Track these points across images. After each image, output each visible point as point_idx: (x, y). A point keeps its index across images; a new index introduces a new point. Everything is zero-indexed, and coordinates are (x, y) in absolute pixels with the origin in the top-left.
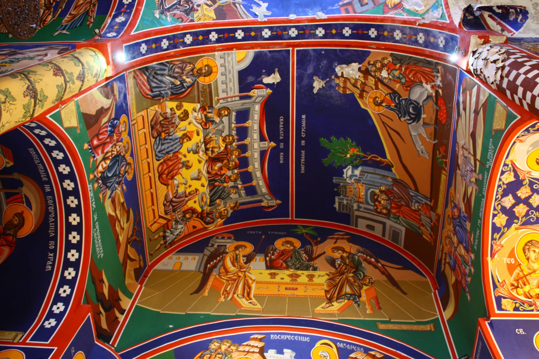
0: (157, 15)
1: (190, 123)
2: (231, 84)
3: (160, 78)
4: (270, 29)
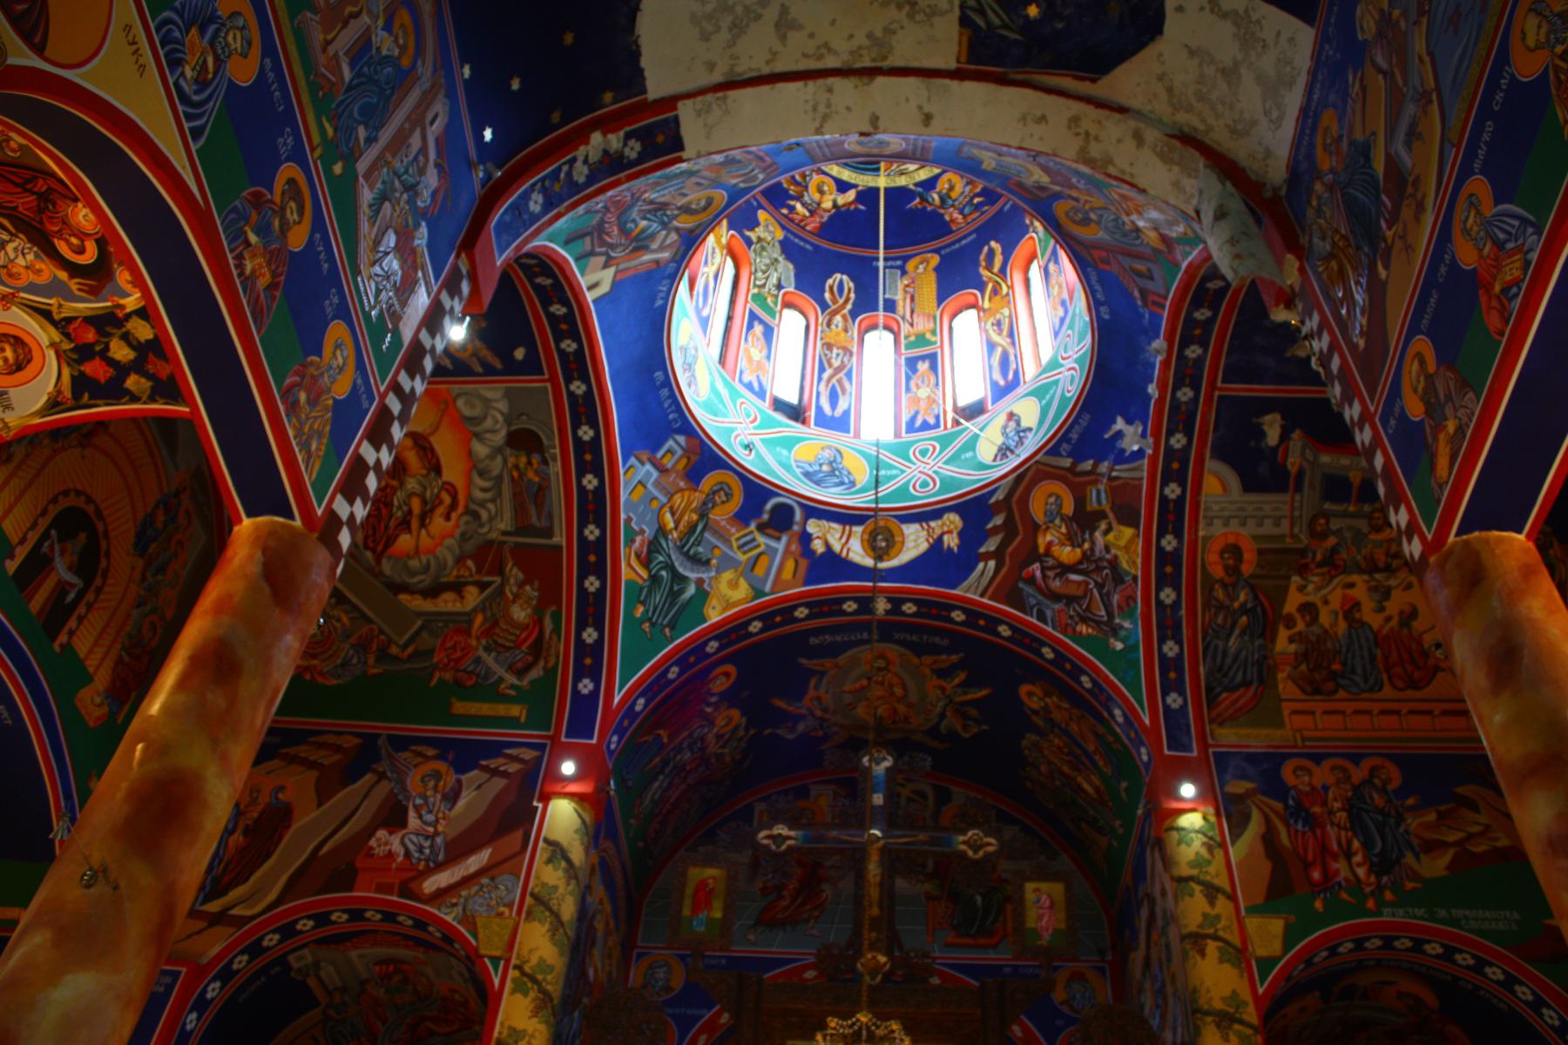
0: (1119, 646)
1: (1326, 602)
2: (1267, 508)
3: (1228, 661)
4: (1170, 433)
